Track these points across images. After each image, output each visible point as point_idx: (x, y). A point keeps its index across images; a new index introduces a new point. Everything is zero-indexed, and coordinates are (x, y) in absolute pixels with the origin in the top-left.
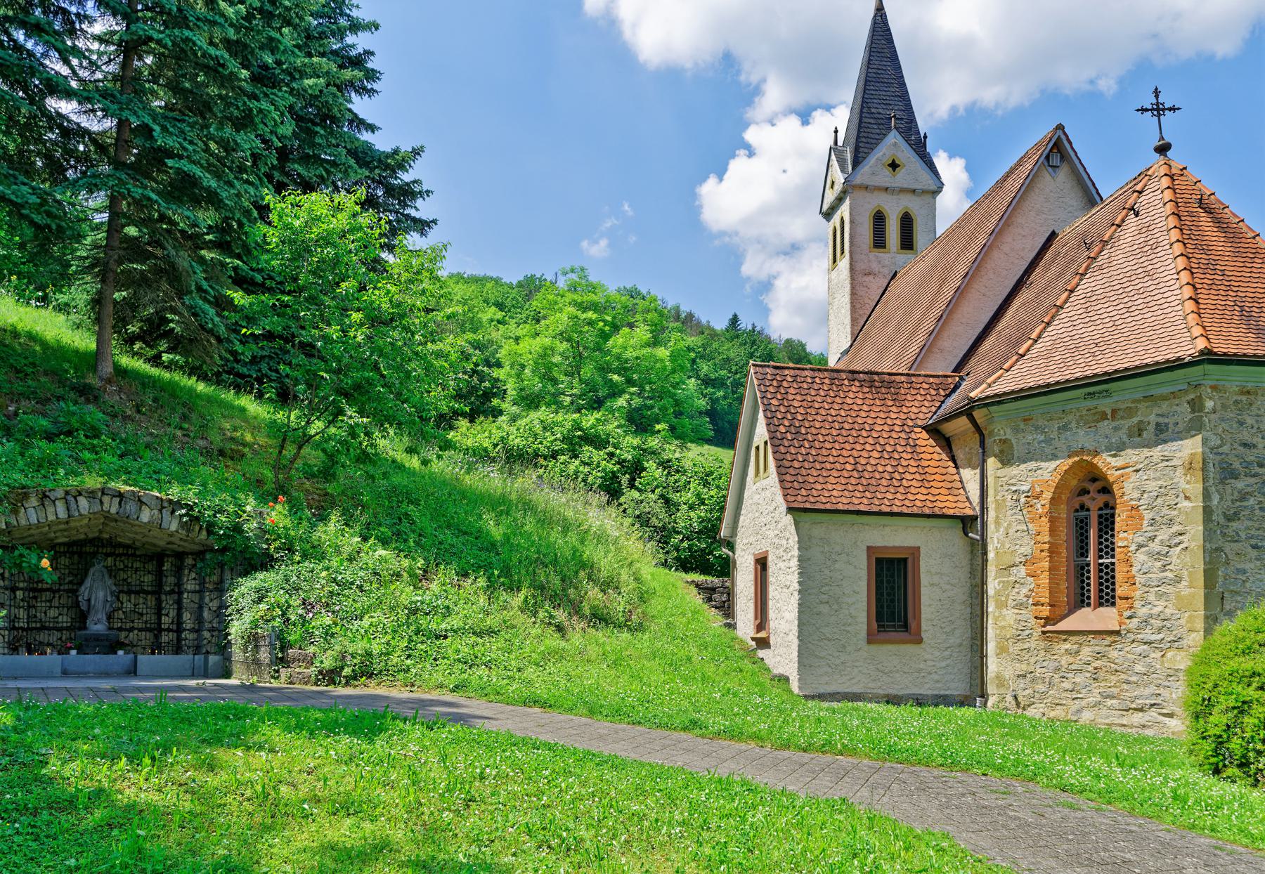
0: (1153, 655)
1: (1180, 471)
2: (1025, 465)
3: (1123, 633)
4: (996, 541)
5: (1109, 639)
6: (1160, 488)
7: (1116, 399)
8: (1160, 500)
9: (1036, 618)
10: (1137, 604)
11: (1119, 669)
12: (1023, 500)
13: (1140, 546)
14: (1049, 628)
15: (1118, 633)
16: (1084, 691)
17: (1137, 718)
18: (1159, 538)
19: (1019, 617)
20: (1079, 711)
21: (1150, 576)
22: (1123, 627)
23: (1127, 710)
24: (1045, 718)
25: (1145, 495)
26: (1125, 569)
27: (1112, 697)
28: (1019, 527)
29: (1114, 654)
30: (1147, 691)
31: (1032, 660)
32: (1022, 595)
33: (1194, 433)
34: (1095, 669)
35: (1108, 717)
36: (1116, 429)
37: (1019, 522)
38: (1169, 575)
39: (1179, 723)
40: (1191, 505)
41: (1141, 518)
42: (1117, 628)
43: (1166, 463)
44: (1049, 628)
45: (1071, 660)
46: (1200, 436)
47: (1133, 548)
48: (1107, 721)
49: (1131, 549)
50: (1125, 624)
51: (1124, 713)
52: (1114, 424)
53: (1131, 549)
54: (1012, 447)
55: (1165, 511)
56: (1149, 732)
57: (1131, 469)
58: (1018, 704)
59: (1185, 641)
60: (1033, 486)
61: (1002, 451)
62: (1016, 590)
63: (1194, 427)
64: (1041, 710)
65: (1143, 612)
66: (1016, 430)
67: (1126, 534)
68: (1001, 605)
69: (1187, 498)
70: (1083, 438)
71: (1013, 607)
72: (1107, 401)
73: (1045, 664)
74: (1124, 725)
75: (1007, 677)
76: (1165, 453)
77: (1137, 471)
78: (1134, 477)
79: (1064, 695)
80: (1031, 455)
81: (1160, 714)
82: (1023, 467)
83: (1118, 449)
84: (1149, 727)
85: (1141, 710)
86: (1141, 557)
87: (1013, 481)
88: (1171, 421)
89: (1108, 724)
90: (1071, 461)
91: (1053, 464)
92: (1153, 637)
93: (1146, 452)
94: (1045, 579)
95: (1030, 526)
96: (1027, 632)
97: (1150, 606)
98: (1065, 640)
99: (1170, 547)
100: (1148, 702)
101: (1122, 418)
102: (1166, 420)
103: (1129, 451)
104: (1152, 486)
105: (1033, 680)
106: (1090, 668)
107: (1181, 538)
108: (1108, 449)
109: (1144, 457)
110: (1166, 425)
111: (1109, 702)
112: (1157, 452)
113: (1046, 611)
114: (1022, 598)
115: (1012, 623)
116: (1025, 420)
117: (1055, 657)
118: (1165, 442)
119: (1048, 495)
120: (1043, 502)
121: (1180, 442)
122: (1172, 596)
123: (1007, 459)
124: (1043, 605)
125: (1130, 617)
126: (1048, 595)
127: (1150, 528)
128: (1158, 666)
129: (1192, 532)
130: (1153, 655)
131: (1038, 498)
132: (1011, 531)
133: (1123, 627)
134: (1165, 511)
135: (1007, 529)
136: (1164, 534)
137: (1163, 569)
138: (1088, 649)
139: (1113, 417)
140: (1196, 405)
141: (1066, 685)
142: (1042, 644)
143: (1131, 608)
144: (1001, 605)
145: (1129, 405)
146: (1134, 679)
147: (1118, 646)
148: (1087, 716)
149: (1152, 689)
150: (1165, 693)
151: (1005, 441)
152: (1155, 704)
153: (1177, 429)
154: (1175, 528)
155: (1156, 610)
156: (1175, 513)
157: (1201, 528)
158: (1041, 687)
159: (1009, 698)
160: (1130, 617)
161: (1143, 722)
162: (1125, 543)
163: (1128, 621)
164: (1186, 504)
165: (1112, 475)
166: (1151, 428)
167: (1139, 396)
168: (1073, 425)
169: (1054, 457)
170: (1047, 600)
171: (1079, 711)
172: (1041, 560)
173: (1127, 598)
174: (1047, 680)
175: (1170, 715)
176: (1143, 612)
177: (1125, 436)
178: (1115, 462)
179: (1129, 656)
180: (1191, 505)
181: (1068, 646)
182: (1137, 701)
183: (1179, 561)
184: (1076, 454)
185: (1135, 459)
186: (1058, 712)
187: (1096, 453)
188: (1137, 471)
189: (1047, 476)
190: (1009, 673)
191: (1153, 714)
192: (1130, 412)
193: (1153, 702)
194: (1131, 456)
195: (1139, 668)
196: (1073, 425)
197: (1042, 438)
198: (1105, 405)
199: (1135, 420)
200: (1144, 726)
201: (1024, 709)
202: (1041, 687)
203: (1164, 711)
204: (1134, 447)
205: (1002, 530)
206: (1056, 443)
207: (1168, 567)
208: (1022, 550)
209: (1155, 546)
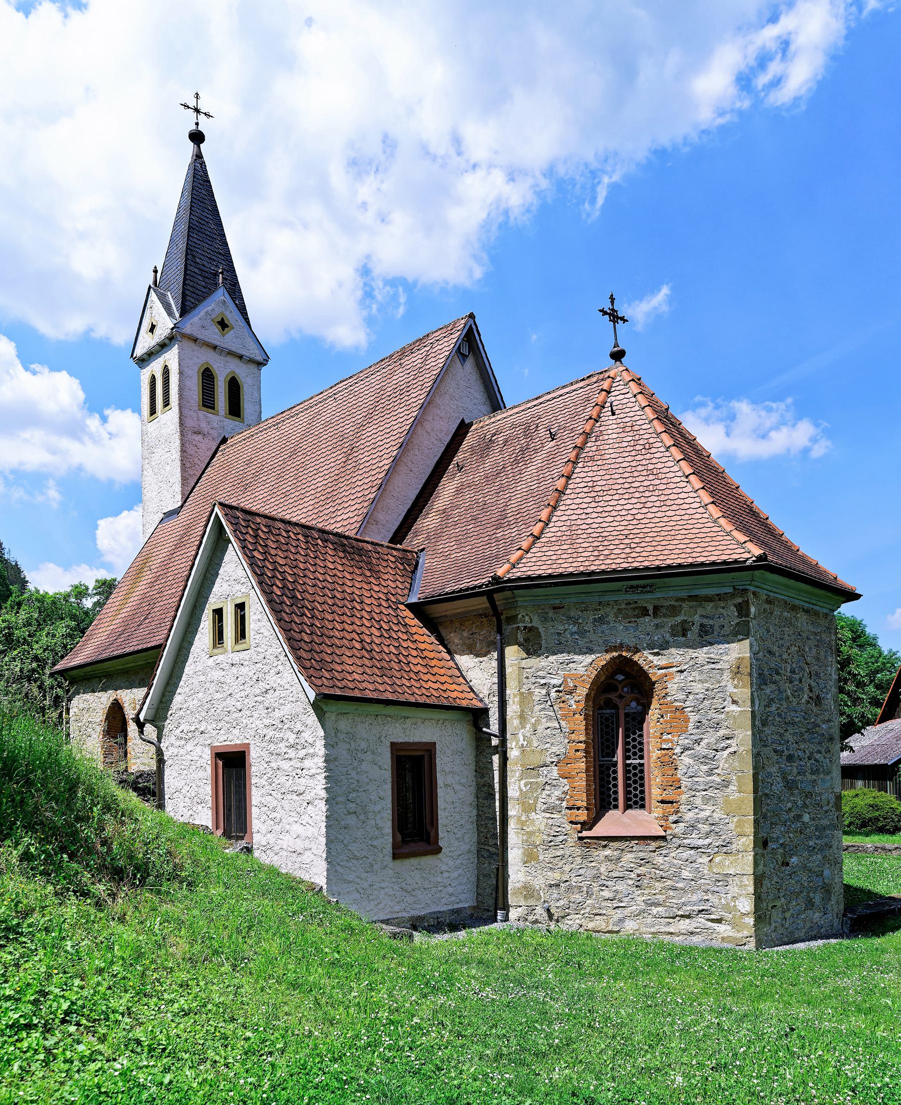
0: (701, 860)
1: (727, 675)
2: (555, 657)
3: (669, 838)
4: (521, 738)
5: (654, 845)
6: (707, 690)
7: (659, 595)
8: (706, 703)
9: (571, 822)
10: (683, 808)
11: (664, 875)
12: (553, 694)
13: (686, 749)
14: (585, 834)
15: (663, 838)
16: (626, 899)
17: (684, 925)
18: (706, 741)
19: (550, 822)
20: (621, 920)
21: (696, 779)
22: (669, 832)
23: (674, 918)
24: (582, 930)
25: (691, 697)
26: (670, 773)
27: (657, 905)
28: (549, 724)
29: (659, 860)
30: (695, 898)
31: (567, 868)
32: (554, 798)
33: (741, 637)
34: (639, 875)
35: (653, 926)
36: (657, 626)
37: (550, 718)
38: (717, 779)
39: (729, 928)
40: (739, 709)
41: (687, 720)
42: (663, 834)
43: (713, 666)
44: (585, 834)
45: (611, 867)
46: (748, 641)
47: (678, 750)
48: (652, 930)
49: (676, 751)
50: (670, 828)
51: (671, 920)
52: (656, 621)
53: (676, 751)
54: (540, 636)
55: (712, 714)
56: (696, 939)
57: (675, 669)
58: (550, 916)
59: (734, 846)
60: (565, 681)
61: (527, 640)
62: (548, 793)
63: (739, 633)
64: (578, 921)
65: (689, 816)
66: (545, 619)
67: (670, 736)
68: (529, 809)
69: (734, 702)
70: (622, 633)
71: (544, 811)
72: (649, 596)
73: (582, 872)
74: (672, 933)
75: (538, 888)
76: (712, 656)
77: (681, 672)
78: (678, 678)
79: (604, 904)
80: (562, 646)
81: (708, 920)
82: (552, 658)
83: (662, 647)
84: (698, 933)
85: (689, 917)
86: (686, 760)
87: (540, 673)
88: (716, 623)
89: (653, 933)
90: (608, 656)
91: (589, 658)
92: (700, 842)
93: (691, 653)
94: (581, 782)
95: (563, 723)
96: (561, 838)
97: (696, 810)
98: (605, 846)
99: (717, 750)
100: (695, 908)
101: (665, 616)
102: (711, 622)
103: (673, 650)
104: (698, 688)
105: (569, 889)
106: (633, 875)
107: (728, 742)
108: (650, 647)
109: (688, 657)
110: (712, 626)
111: (655, 910)
112: (702, 654)
113: (583, 816)
114: (553, 800)
115: (543, 828)
116: (554, 608)
117: (593, 864)
118: (711, 644)
119: (583, 691)
120: (577, 699)
121: (727, 646)
122: (721, 800)
123: (532, 648)
124: (578, 809)
125: (676, 822)
126: (585, 798)
127: (695, 731)
128: (706, 872)
129: (741, 736)
130: (701, 860)
131: (571, 693)
132: (541, 728)
133: (669, 832)
134: (712, 714)
135: (534, 725)
136: (710, 738)
137: (710, 773)
138: (632, 855)
139: (655, 614)
140: (742, 610)
141: (606, 894)
142: (578, 851)
143: (677, 812)
144: (529, 809)
145: (673, 603)
146: (680, 885)
147: (664, 852)
148: (630, 926)
149: (700, 895)
150: (714, 899)
151: (531, 629)
152: (703, 910)
153: (723, 632)
154: (722, 732)
155: (702, 815)
156: (723, 716)
157: (749, 733)
158: (578, 897)
159: (540, 911)
160: (676, 822)
161: (691, 929)
162: (670, 745)
163: (674, 826)
164: (734, 707)
165: (655, 674)
166: (696, 629)
167: (684, 594)
168: (611, 618)
169: (590, 651)
170: (585, 804)
171: (621, 920)
172: (576, 760)
173: (672, 803)
174: (585, 889)
175: (719, 921)
176: (689, 816)
177: (668, 635)
178: (657, 661)
179: (676, 862)
180: (739, 709)
181: (608, 852)
182: (684, 907)
183: (727, 766)
184: (615, 649)
185: (679, 659)
186: (599, 923)
187: (637, 651)
188: (681, 672)
189: (581, 670)
190: (539, 882)
191: (701, 920)
192: (674, 611)
193: (701, 908)
194: (675, 655)
195: (685, 874)
196: (611, 618)
197: (575, 629)
198: (646, 600)
199: (679, 619)
200: (692, 933)
201: (557, 921)
202: (578, 897)
203: (713, 917)
204: (678, 646)
205: (528, 726)
206: (591, 636)
207: (716, 771)
208: (554, 749)
209: (701, 749)
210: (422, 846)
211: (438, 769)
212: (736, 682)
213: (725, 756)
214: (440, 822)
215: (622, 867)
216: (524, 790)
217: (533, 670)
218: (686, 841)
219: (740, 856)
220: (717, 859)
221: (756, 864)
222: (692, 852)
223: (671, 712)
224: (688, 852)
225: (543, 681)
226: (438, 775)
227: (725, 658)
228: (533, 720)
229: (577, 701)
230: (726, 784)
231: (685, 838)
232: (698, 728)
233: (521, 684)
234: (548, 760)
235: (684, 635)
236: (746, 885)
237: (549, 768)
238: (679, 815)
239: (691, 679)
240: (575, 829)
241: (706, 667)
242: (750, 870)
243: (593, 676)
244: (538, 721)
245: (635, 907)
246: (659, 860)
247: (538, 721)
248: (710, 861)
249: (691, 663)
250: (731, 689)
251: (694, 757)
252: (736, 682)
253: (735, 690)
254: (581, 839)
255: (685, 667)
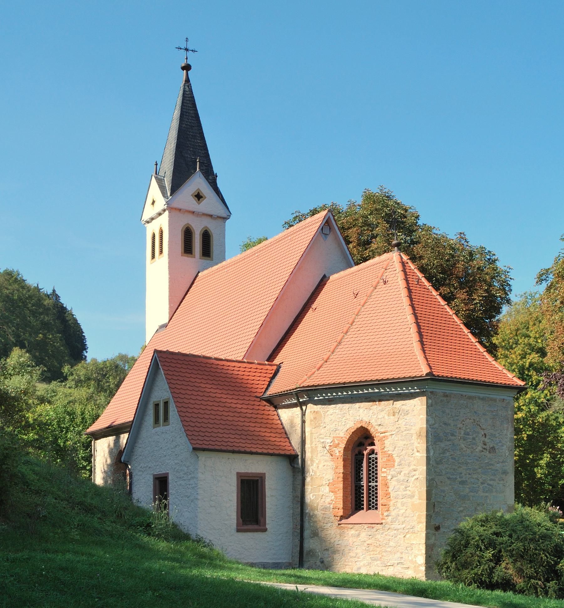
1: (414, 437)
6: (404, 445)
8: (404, 452)
10: (391, 509)
21: (398, 493)
28: (325, 463)
34: (368, 545)
41: (394, 461)
43: (408, 432)
47: (389, 477)
67: (385, 470)
69: (418, 451)
71: (321, 510)
76: (407, 426)
92: (399, 527)
94: (340, 494)
97: (398, 510)
104: (401, 443)
107: (415, 473)
119: (343, 446)
125: (387, 516)
127: (398, 467)
129: (421, 470)
136: (406, 470)
146: (389, 549)
147: (381, 532)
149: (398, 555)
156: (412, 459)
157: (425, 468)
162: (385, 475)
163: (386, 518)
164: (418, 454)
170: (342, 506)
189: (342, 435)
193: (399, 562)
203: (405, 566)
210: (256, 527)
211: (267, 487)
212: (419, 441)
213: (413, 480)
214: (267, 515)
215: (360, 540)
216: (312, 499)
217: (318, 434)
218: (392, 526)
219: (419, 534)
220: (408, 536)
221: (428, 538)
222: (395, 532)
223: (387, 457)
224: (394, 532)
225: (322, 441)
226: (267, 490)
227: (413, 428)
228: (317, 462)
229: (339, 451)
230: (412, 496)
231: (391, 525)
232: (399, 466)
233: (311, 443)
234: (324, 483)
235: (394, 415)
236: (421, 549)
237: (324, 487)
238: (389, 512)
239: (397, 439)
240: (337, 519)
241: (404, 433)
242: (424, 541)
243: (348, 437)
244: (320, 462)
245: (366, 561)
246: (378, 537)
247: (320, 462)
248: (404, 537)
249: (397, 431)
250: (416, 444)
251: (398, 481)
252: (419, 441)
253: (418, 445)
254: (339, 524)
255: (394, 433)
